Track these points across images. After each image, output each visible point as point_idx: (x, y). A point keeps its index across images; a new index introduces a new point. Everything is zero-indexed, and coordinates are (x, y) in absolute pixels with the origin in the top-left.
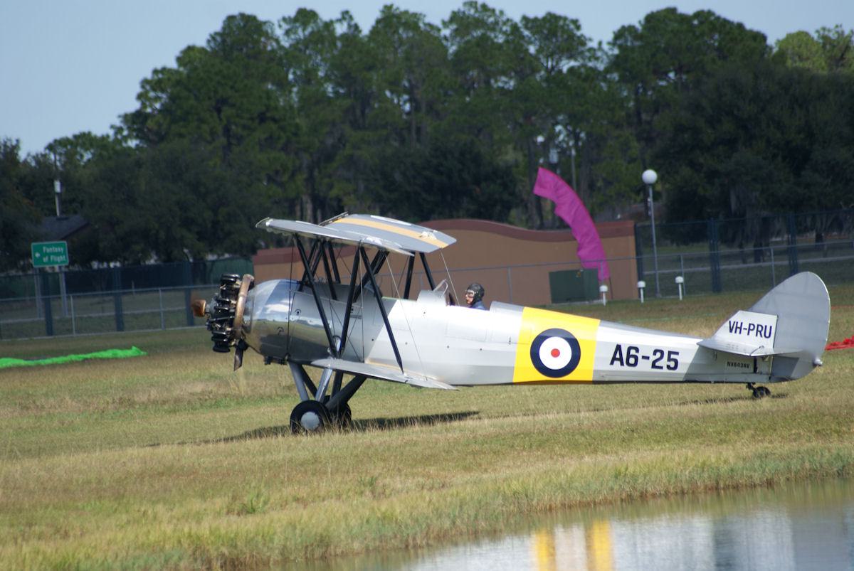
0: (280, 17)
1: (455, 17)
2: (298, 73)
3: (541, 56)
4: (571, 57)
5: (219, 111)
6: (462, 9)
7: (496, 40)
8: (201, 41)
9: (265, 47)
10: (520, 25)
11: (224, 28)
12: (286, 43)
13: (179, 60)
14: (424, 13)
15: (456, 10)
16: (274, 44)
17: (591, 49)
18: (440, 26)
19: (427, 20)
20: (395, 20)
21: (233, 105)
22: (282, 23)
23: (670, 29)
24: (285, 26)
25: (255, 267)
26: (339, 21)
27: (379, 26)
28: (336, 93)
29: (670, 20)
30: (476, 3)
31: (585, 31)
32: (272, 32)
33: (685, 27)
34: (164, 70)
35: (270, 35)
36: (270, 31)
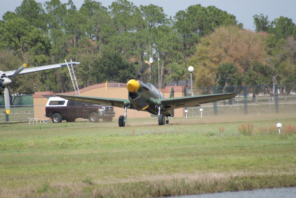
0: (45, 2)
2: (51, 24)
3: (147, 21)
4: (159, 22)
5: (19, 37)
7: (129, 14)
8: (13, 10)
10: (139, 8)
11: (22, 5)
12: (46, 12)
13: (3, 17)
14: (101, 2)
15: (114, 2)
16: (42, 12)
17: (166, 19)
18: (108, 7)
19: (102, 5)
20: (90, 5)
21: (24, 35)
22: (46, 4)
23: (198, 12)
25: (34, 99)
26: (67, 4)
27: (84, 7)
28: (66, 32)
29: (198, 9)
31: (165, 12)
32: (41, 8)
33: (204, 12)
35: (40, 8)
36: (40, 7)
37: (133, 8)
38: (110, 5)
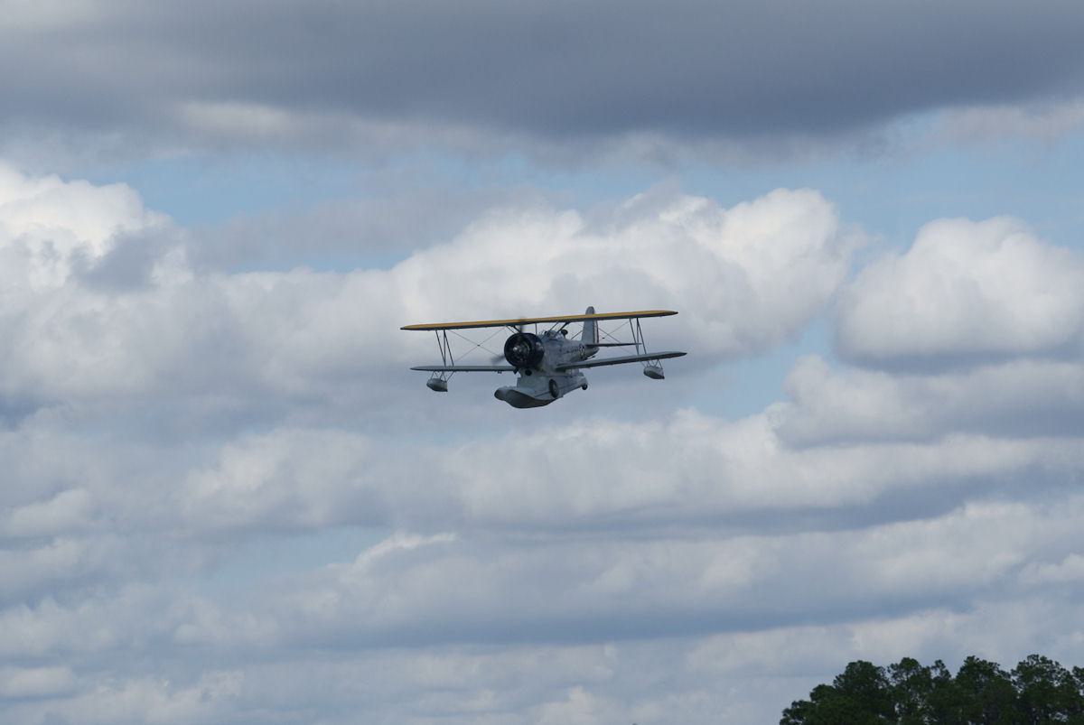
0: (889, 665)
1: (1022, 666)
2: (903, 706)
6: (1027, 661)
8: (829, 682)
9: (877, 687)
10: (1072, 674)
11: (847, 672)
13: (812, 695)
15: (1022, 661)
16: (884, 684)
19: (1000, 668)
20: (975, 668)
24: (893, 671)
26: (933, 667)
30: (1038, 656)
34: (801, 703)
37: (1059, 673)
38: (1015, 669)
